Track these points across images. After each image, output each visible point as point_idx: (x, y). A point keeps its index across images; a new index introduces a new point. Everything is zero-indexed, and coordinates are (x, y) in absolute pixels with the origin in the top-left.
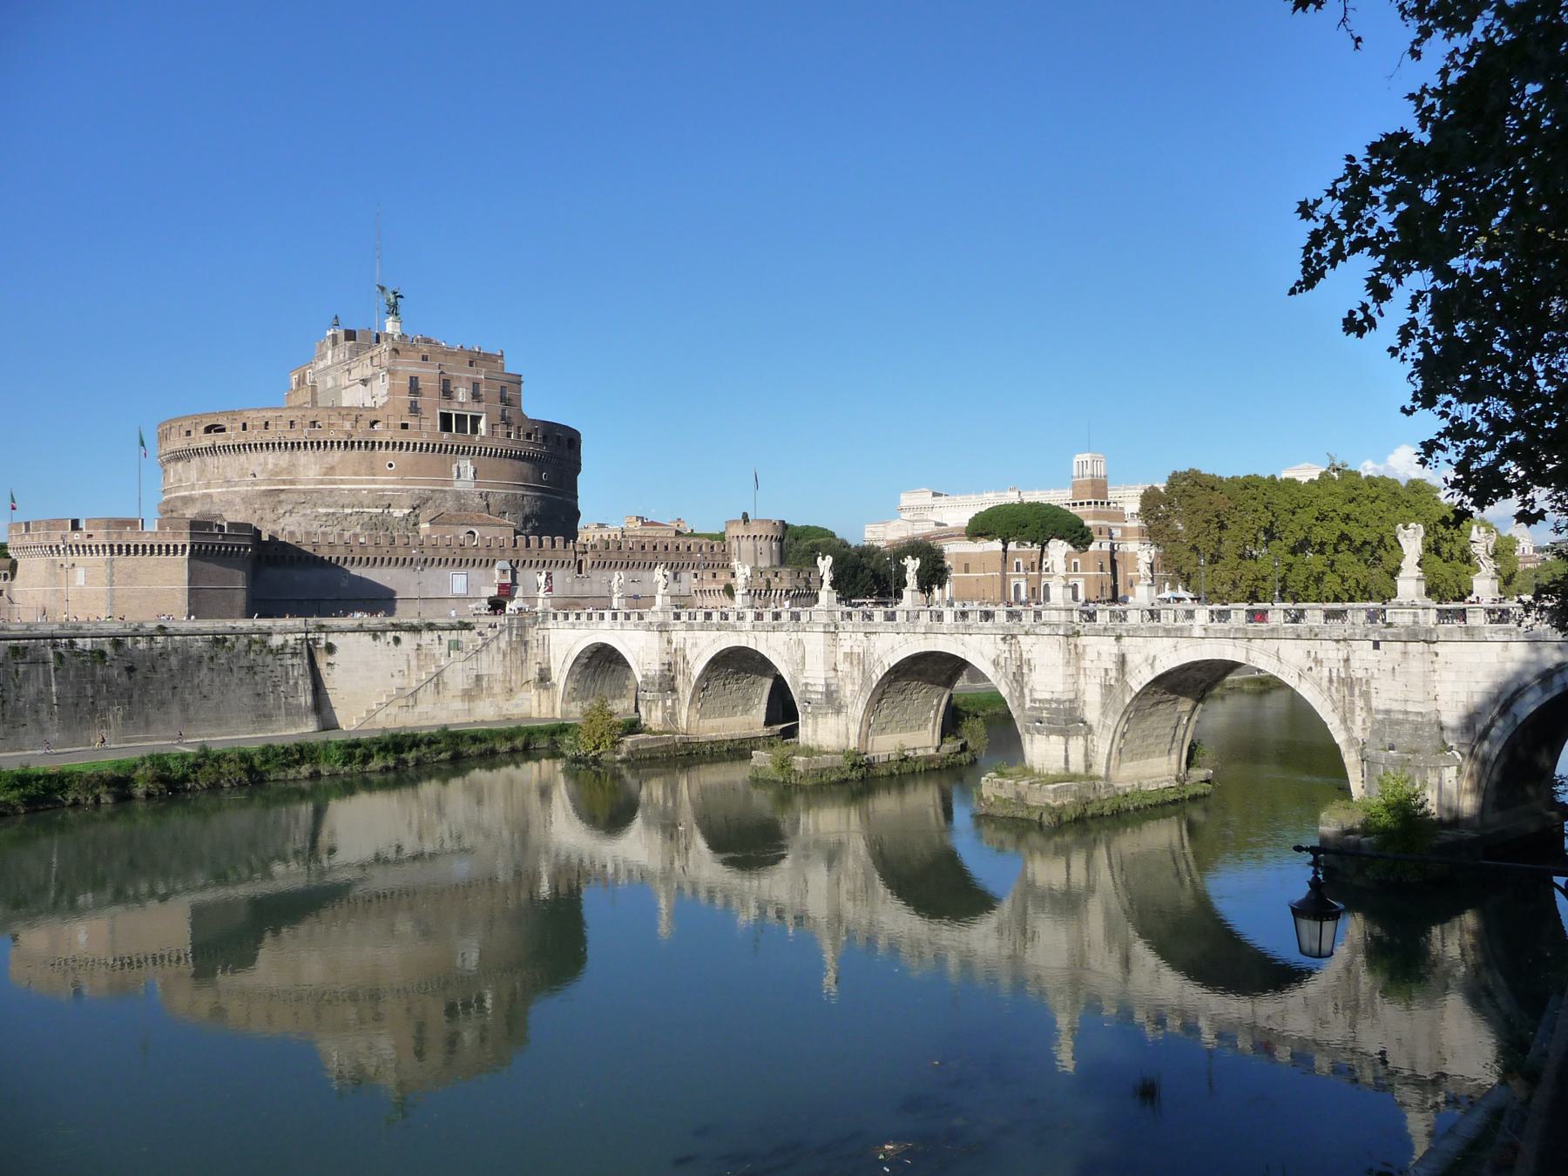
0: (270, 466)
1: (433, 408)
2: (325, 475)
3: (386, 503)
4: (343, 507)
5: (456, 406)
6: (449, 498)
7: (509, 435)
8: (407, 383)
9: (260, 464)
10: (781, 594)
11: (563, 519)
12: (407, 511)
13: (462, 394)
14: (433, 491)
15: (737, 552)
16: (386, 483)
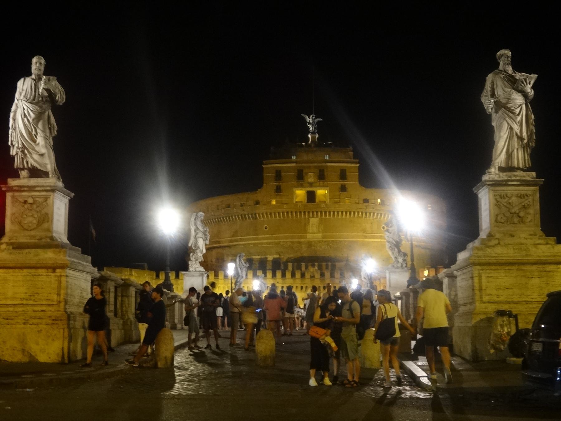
2: (233, 237)
6: (303, 246)
8: (274, 175)
13: (311, 177)
14: (292, 242)
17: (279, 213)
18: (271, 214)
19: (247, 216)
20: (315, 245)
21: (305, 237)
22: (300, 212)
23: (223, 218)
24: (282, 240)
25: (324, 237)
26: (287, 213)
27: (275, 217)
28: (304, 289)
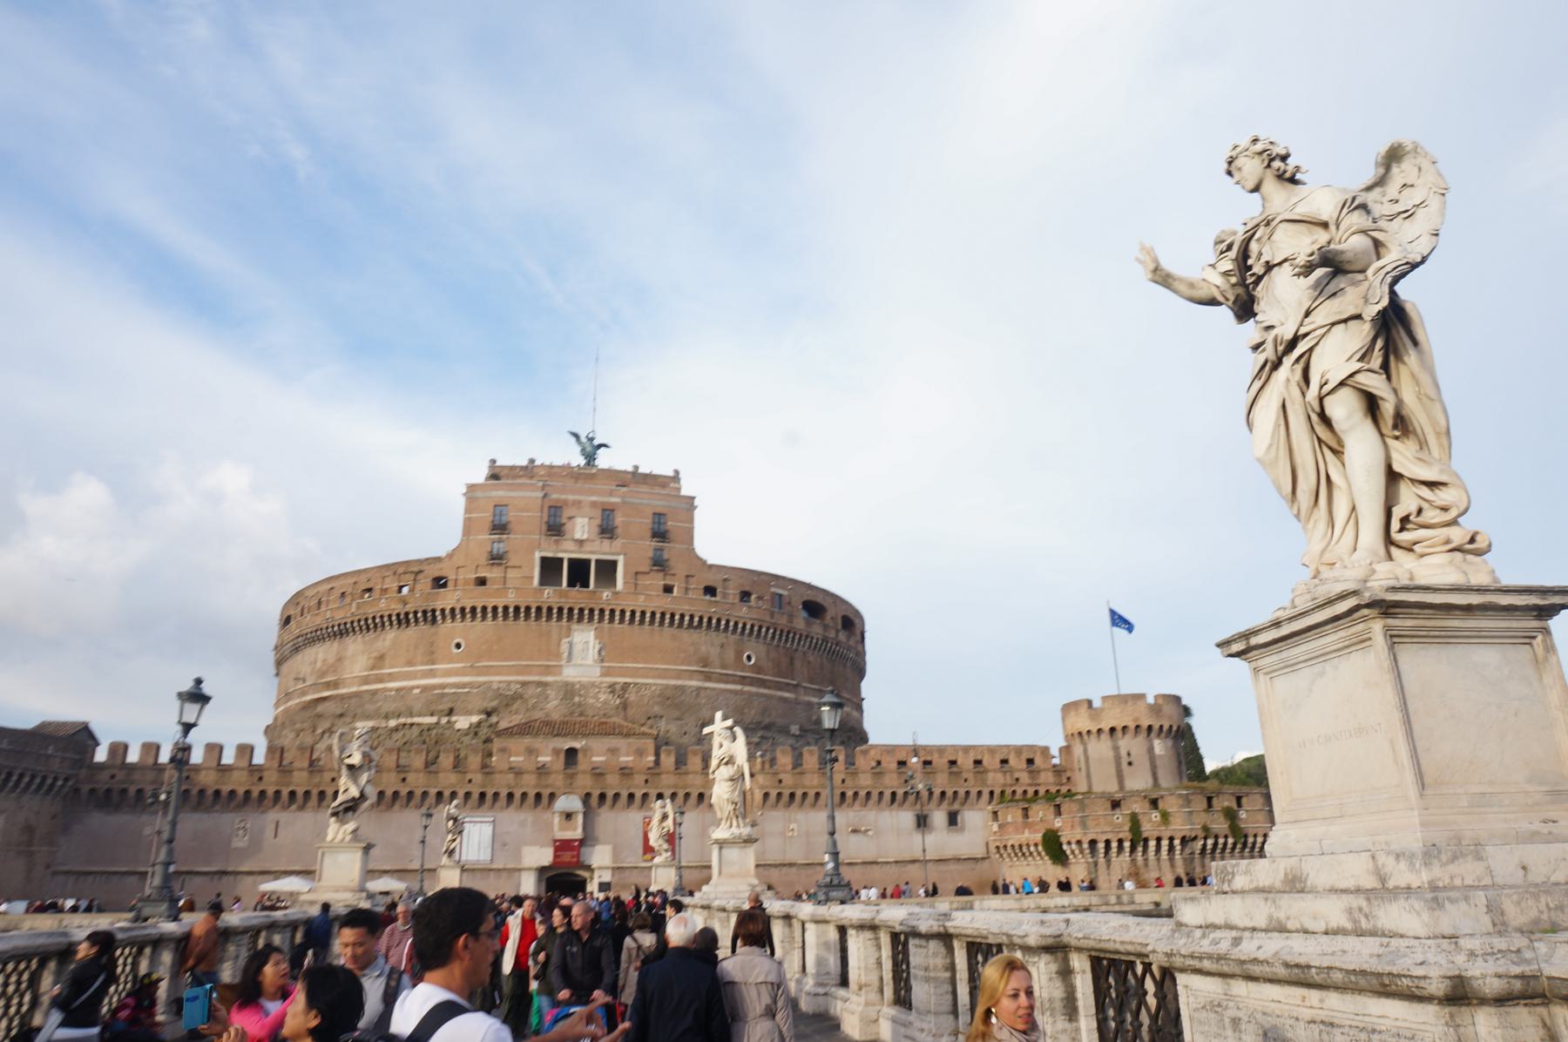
0: (319, 664)
1: (530, 552)
2: (372, 669)
3: (446, 706)
4: (387, 717)
5: (569, 545)
6: (551, 693)
7: (668, 589)
9: (311, 664)
10: (1171, 848)
11: (795, 729)
12: (475, 719)
13: (581, 527)
14: (524, 684)
15: (1084, 768)
16: (448, 675)
17: (495, 609)
18: (473, 609)
19: (411, 616)
20: (582, 692)
21: (557, 670)
22: (550, 609)
23: (352, 622)
24: (498, 678)
25: (606, 672)
26: (517, 609)
27: (484, 617)
28: (545, 800)
